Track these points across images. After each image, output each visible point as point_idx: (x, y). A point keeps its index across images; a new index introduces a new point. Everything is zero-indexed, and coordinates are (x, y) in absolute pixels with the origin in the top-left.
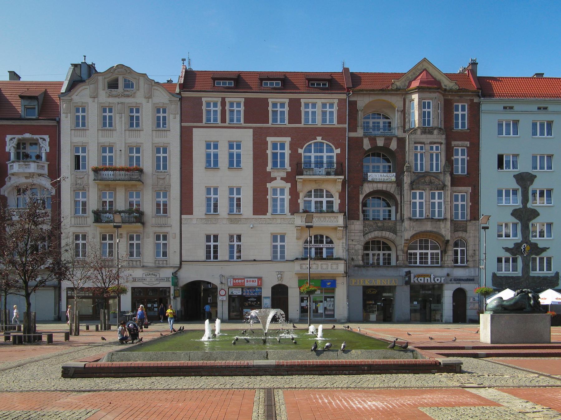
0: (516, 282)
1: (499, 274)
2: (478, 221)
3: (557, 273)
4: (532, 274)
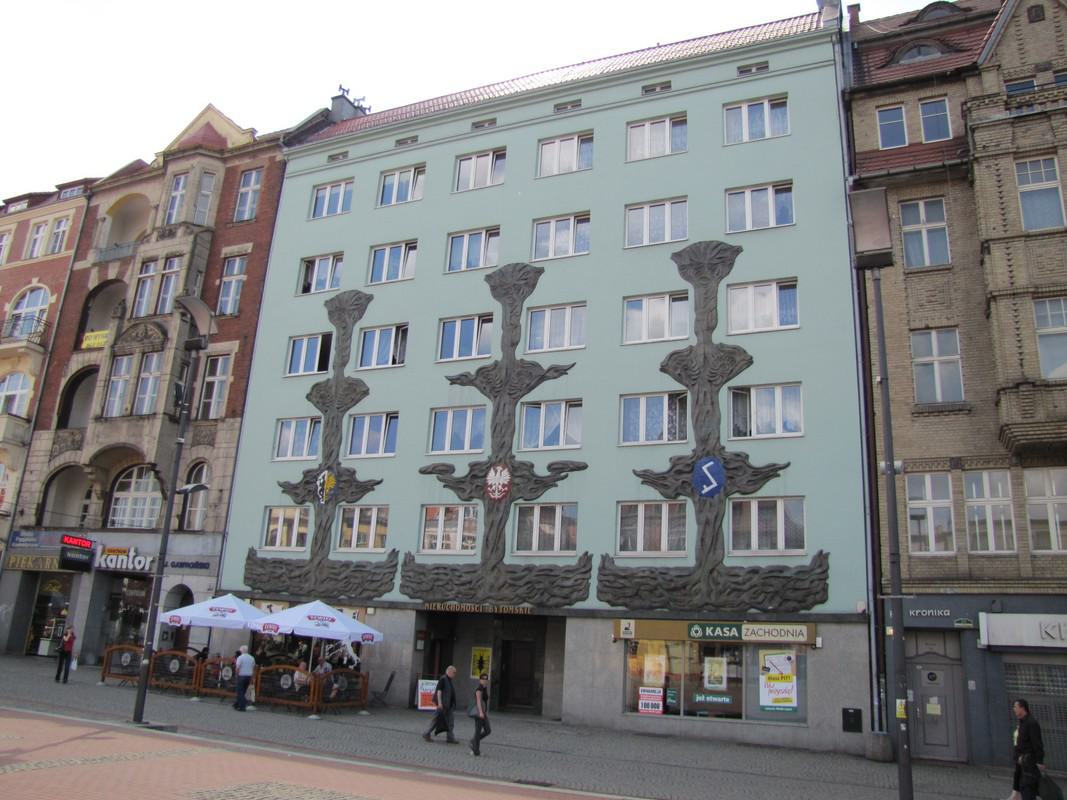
0: (293, 574)
1: (267, 553)
2: (239, 419)
3: (822, 559)
4: (734, 558)
